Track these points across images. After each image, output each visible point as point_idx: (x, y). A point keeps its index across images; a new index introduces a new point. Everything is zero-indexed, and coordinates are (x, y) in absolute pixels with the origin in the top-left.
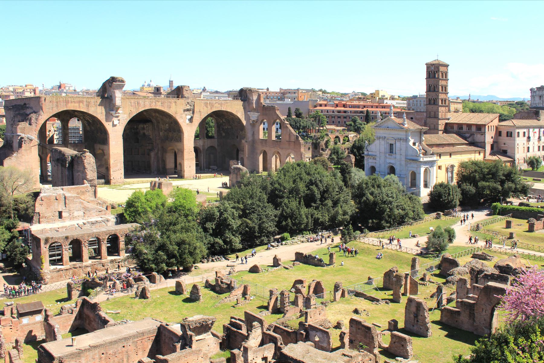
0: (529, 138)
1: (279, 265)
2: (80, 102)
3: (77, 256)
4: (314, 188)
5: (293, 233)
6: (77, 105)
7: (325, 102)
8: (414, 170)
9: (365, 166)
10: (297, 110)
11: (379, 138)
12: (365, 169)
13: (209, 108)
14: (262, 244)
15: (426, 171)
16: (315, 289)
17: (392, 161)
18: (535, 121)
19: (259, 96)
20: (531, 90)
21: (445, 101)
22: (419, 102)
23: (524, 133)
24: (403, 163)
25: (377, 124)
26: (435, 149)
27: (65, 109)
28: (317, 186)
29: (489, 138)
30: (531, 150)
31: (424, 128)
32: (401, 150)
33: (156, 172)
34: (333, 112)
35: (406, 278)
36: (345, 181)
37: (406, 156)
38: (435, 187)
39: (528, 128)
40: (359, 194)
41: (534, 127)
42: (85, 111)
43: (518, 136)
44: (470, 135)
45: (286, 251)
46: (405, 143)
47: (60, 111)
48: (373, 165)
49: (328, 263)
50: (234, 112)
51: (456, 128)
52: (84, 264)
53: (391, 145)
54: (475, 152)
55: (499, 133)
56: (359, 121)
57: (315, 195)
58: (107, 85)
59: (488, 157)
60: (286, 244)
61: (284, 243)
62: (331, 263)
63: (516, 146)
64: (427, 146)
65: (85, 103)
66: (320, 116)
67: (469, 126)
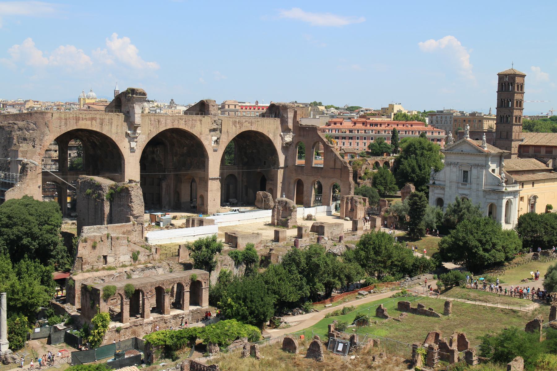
2: (92, 119)
3: (136, 310)
6: (89, 122)
13: (238, 127)
15: (508, 203)
17: (466, 192)
19: (295, 113)
21: (520, 118)
22: (444, 119)
24: (481, 194)
27: (75, 128)
31: (506, 151)
33: (167, 207)
42: (98, 130)
47: (69, 130)
50: (265, 133)
52: (146, 320)
53: (465, 172)
58: (123, 99)
60: (374, 292)
62: (446, 313)
65: (98, 121)
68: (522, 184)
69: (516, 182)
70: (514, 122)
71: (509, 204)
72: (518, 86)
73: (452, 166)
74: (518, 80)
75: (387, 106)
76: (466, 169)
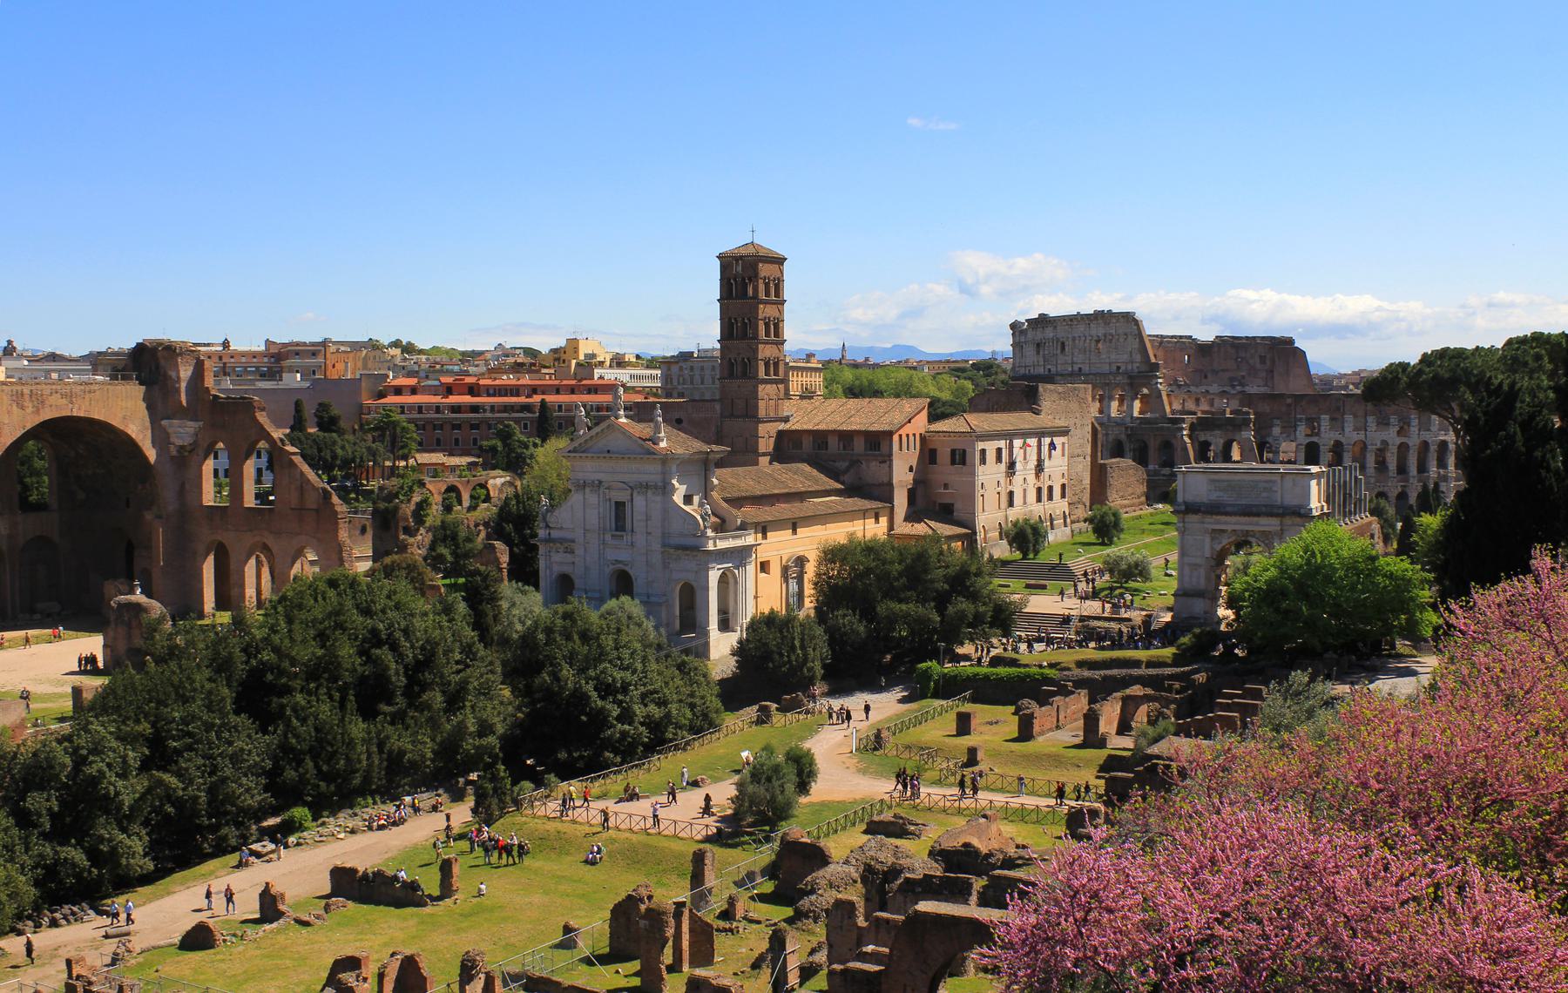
0: (1012, 465)
1: (280, 915)
4: (384, 654)
5: (323, 807)
7: (412, 381)
8: (690, 577)
9: (541, 574)
10: (323, 407)
11: (582, 486)
12: (542, 584)
13: (30, 410)
14: (221, 850)
15: (723, 580)
16: (398, 981)
17: (623, 555)
18: (1028, 415)
20: (1014, 326)
22: (697, 372)
23: (999, 451)
24: (656, 559)
25: (576, 444)
26: (749, 512)
28: (394, 647)
29: (902, 472)
30: (1018, 499)
32: (648, 519)
34: (438, 409)
35: (678, 915)
36: (479, 625)
37: (665, 535)
38: (753, 626)
39: (1009, 436)
40: (526, 662)
41: (1024, 435)
43: (983, 461)
44: (850, 464)
45: (300, 867)
46: (659, 498)
48: (567, 569)
49: (436, 892)
50: (116, 422)
51: (807, 443)
53: (620, 506)
54: (864, 514)
55: (929, 454)
56: (519, 436)
57: (388, 679)
59: (903, 528)
60: (298, 844)
61: (292, 839)
62: (447, 890)
63: (979, 492)
64: (725, 505)
66: (395, 424)
67: (846, 437)
68: (763, 529)
69: (743, 527)
70: (762, 374)
71: (731, 581)
72: (767, 285)
73: (587, 490)
74: (765, 270)
75: (562, 343)
76: (622, 496)
